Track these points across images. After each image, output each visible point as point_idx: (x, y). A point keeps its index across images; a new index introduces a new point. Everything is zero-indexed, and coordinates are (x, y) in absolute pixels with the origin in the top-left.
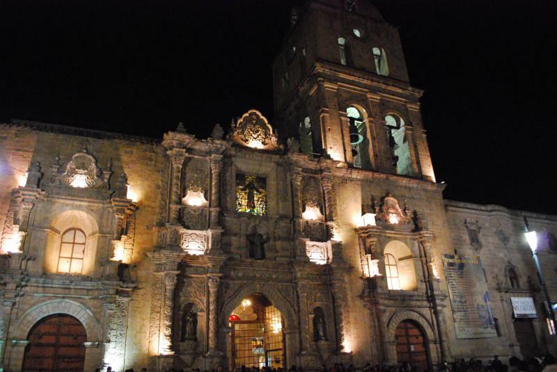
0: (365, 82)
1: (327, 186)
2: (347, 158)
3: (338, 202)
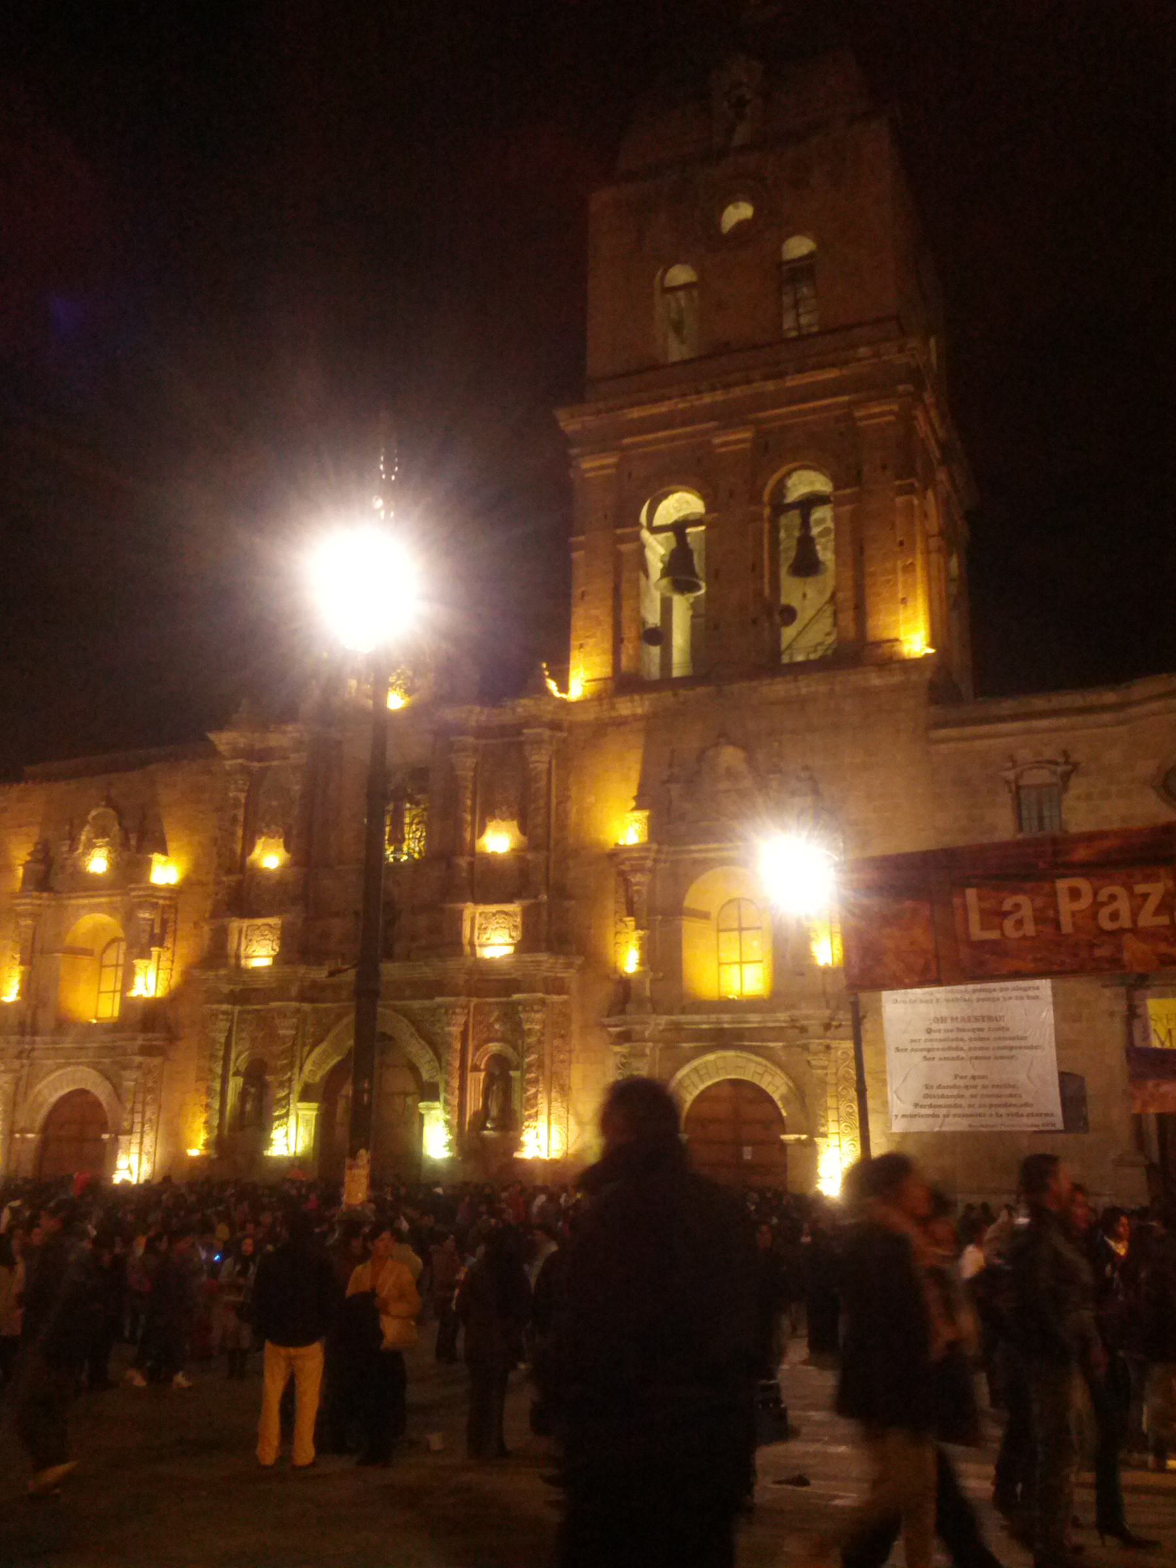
0: (707, 399)
1: (539, 760)
2: (625, 662)
3: (573, 792)
